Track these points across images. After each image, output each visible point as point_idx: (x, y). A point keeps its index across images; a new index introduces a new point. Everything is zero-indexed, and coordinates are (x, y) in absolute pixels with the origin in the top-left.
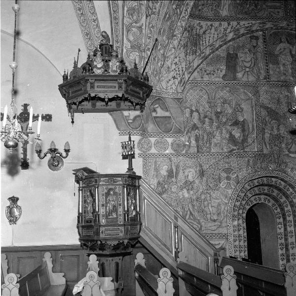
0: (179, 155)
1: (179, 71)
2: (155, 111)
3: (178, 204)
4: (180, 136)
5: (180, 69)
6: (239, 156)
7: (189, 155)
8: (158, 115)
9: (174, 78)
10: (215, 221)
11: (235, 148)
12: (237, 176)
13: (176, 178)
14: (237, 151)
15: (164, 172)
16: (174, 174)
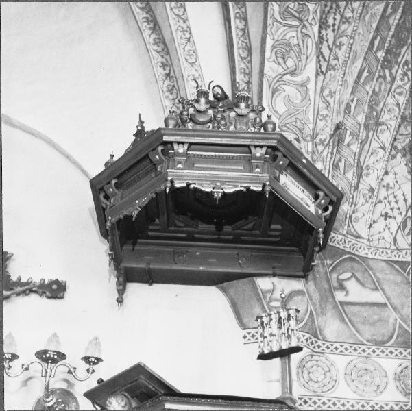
1: (397, 202)
2: (342, 287)
5: (400, 198)
8: (349, 299)
9: (386, 216)
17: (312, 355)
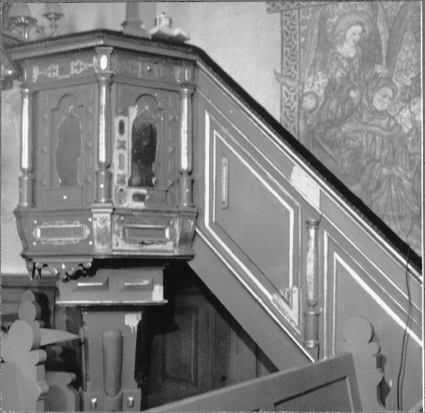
3: (394, 154)
13: (390, 64)
15: (348, 49)
16: (384, 46)
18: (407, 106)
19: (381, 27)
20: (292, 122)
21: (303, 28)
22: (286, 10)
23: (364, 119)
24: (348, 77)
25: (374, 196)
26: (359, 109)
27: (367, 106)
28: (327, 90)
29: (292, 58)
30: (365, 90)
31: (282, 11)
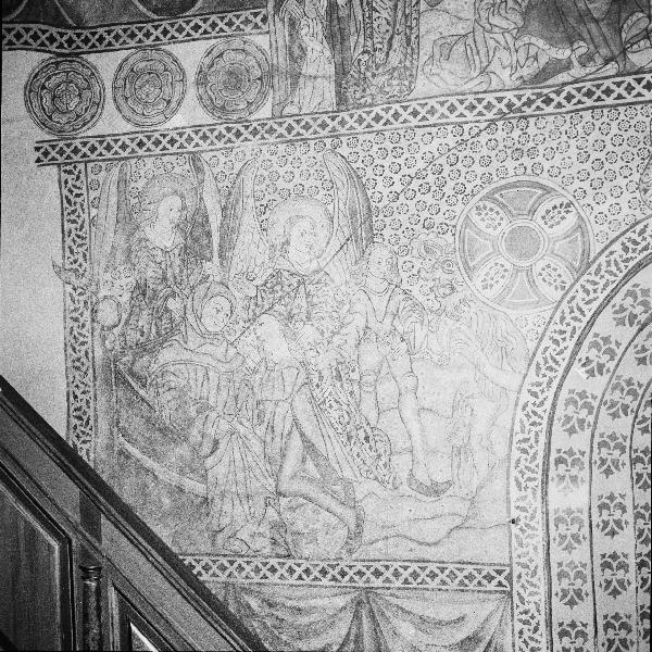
0: (238, 134)
4: (247, 21)
6: (589, 102)
7: (290, 129)
10: (435, 491)
11: (563, 54)
12: (580, 227)
14: (577, 71)
15: (162, 234)
16: (216, 239)
17: (57, 64)
18: (251, 328)
19: (212, 205)
20: (83, 343)
21: (93, 194)
22: (66, 164)
23: (191, 345)
24: (165, 279)
25: (209, 462)
26: (182, 329)
27: (195, 325)
28: (135, 295)
29: (79, 241)
30: (190, 299)
31: (59, 165)
